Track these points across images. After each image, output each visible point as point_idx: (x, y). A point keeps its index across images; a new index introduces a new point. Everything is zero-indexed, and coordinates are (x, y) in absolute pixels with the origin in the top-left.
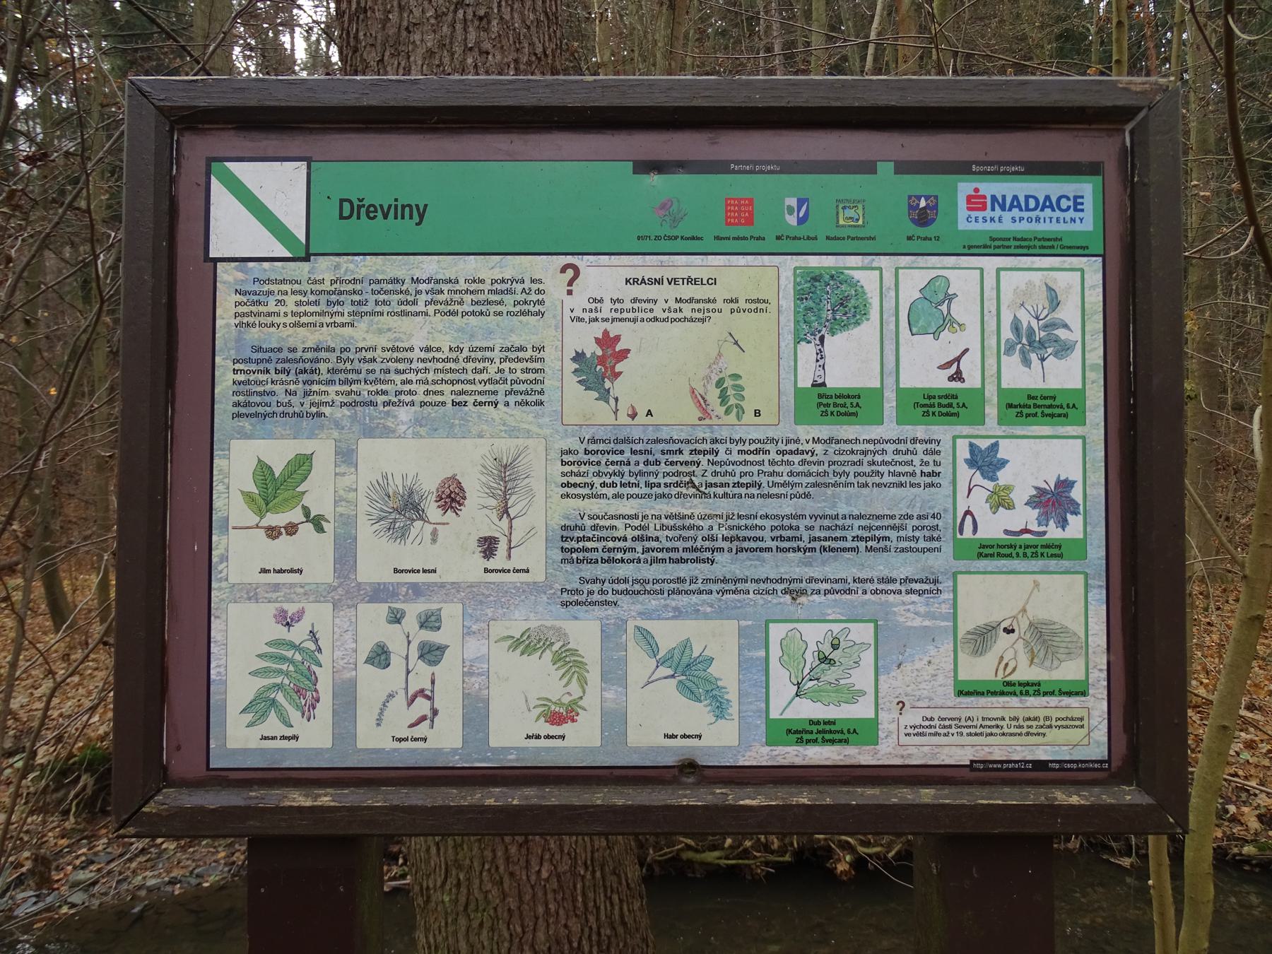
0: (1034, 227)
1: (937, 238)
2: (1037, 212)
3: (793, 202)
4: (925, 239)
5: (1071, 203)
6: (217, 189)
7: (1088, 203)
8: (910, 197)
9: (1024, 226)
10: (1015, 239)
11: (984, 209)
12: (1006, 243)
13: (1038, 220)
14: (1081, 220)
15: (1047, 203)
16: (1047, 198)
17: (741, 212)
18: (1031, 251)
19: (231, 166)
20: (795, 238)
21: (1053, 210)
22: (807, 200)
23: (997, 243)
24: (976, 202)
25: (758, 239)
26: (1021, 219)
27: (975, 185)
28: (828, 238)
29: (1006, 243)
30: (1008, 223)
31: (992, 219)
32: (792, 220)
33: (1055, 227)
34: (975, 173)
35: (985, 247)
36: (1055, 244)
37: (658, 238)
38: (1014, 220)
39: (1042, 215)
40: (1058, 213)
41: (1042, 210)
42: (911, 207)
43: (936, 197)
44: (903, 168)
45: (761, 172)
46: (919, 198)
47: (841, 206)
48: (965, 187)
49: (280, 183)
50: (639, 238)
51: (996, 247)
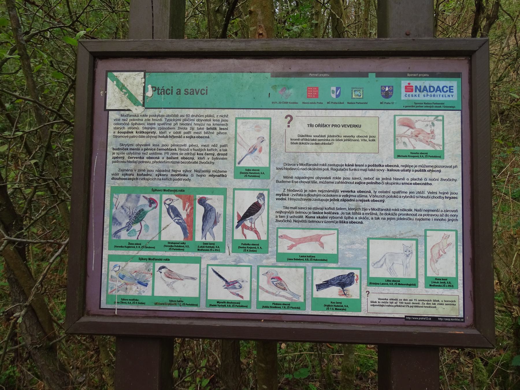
0: (433, 98)
1: (393, 103)
2: (434, 93)
3: (334, 89)
4: (388, 103)
5: (448, 89)
7: (455, 90)
8: (382, 87)
9: (428, 98)
10: (425, 103)
11: (412, 91)
12: (421, 105)
13: (434, 96)
14: (452, 96)
15: (438, 89)
16: (438, 87)
17: (313, 93)
18: (431, 108)
19: (115, 74)
20: (335, 103)
21: (441, 92)
22: (340, 88)
23: (417, 105)
24: (409, 89)
25: (320, 103)
26: (427, 95)
27: (409, 82)
28: (348, 103)
29: (421, 105)
30: (422, 97)
31: (415, 96)
32: (334, 96)
33: (441, 99)
34: (409, 77)
35: (413, 106)
36: (441, 105)
37: (280, 103)
38: (424, 96)
39: (436, 94)
40: (442, 93)
41: (436, 92)
42: (382, 91)
43: (392, 87)
44: (379, 75)
45: (322, 77)
46: (385, 87)
47: (354, 90)
48: (404, 82)
49: (134, 80)
50: (272, 103)
51: (417, 107)
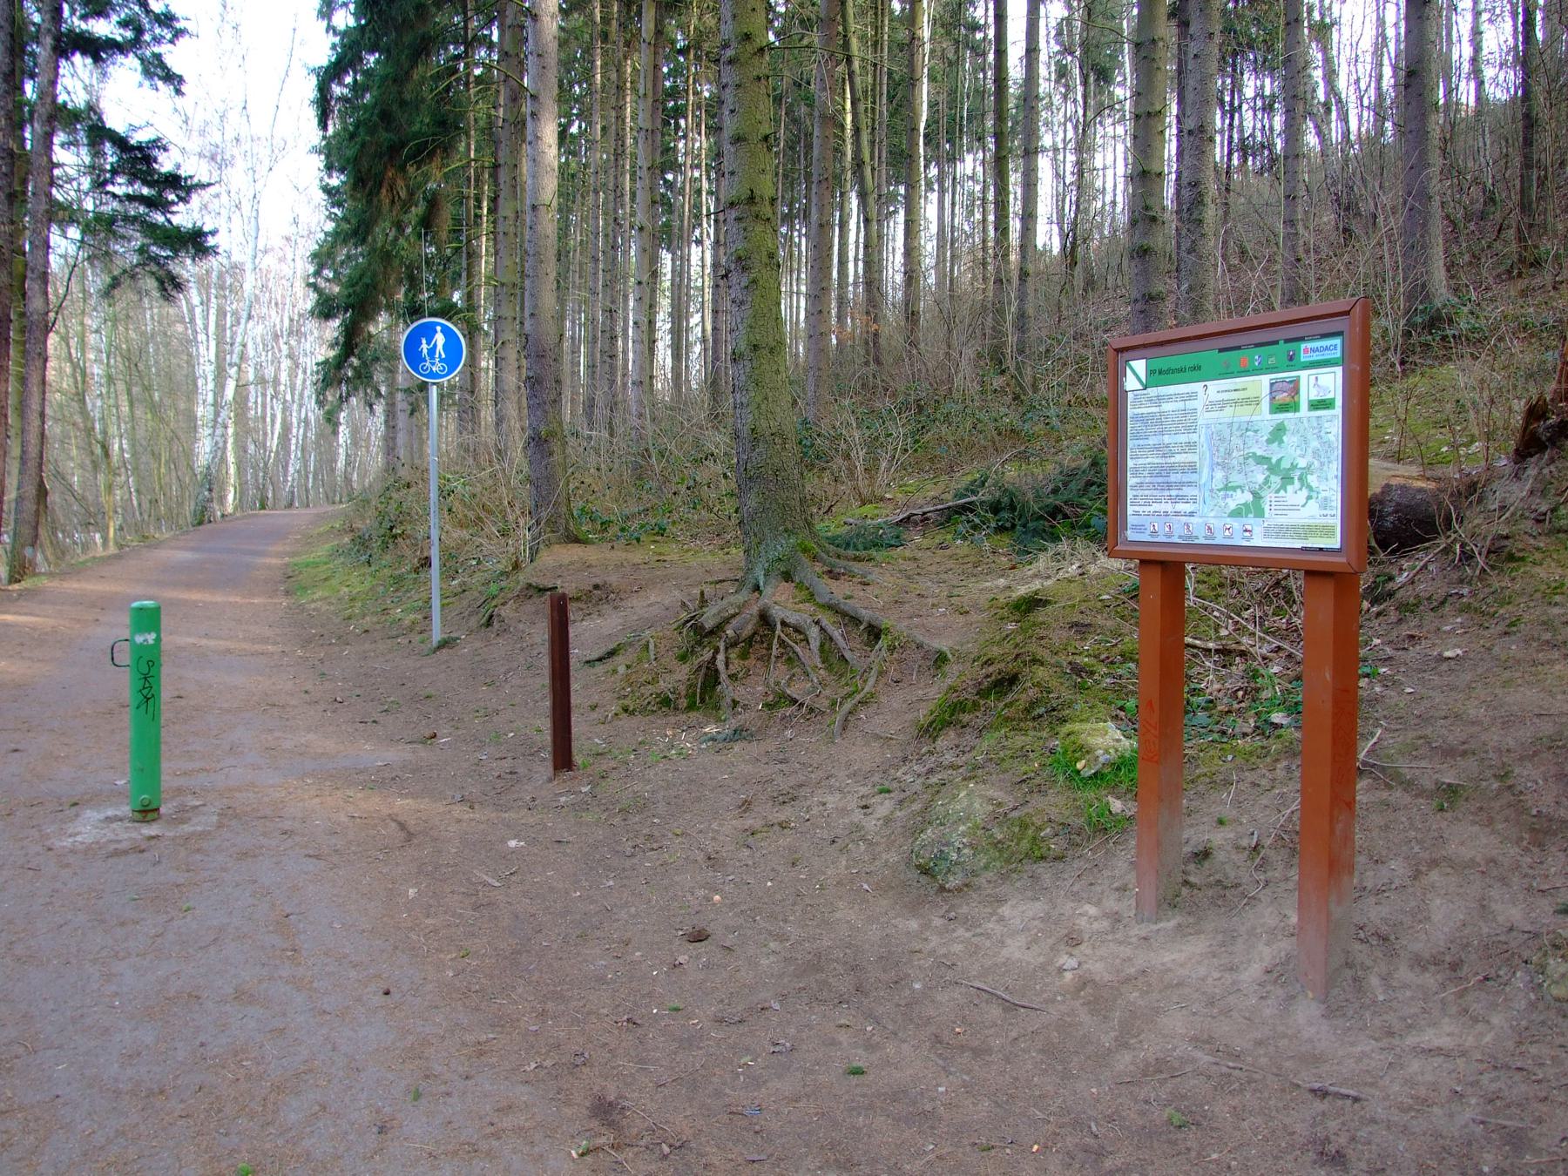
6: (1128, 371)
15: (1327, 348)
24: (1306, 351)
30: (1315, 357)
44: (1287, 341)
48: (1303, 346)
49: (1139, 366)
